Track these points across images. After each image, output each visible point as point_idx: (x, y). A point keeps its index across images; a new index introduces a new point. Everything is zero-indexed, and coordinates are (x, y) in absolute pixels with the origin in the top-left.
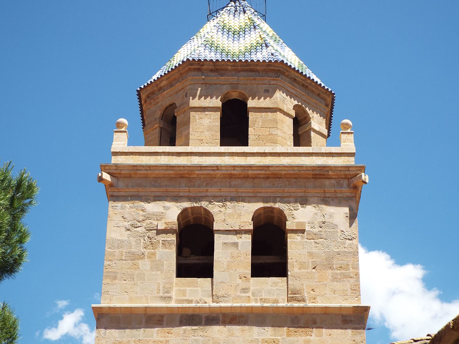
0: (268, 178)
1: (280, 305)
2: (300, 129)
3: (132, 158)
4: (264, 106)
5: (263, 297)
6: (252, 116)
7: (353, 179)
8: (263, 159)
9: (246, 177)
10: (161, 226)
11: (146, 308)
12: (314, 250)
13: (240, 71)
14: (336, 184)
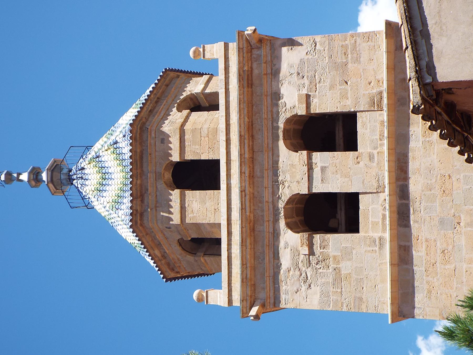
0: (252, 136)
1: (386, 118)
2: (203, 105)
3: (235, 284)
4: (178, 143)
5: (378, 137)
6: (189, 156)
7: (252, 44)
9: (252, 160)
10: (306, 250)
11: (391, 264)
12: (328, 84)
13: (142, 170)
14: (257, 62)
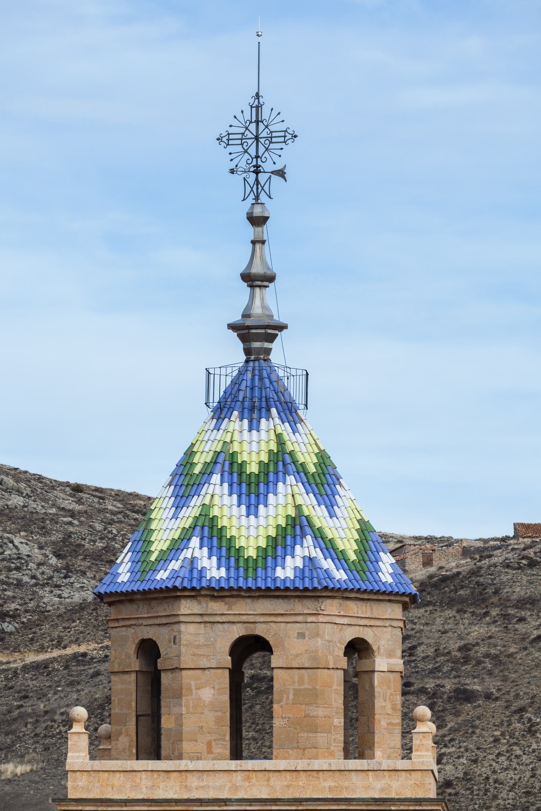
8: (294, 782)
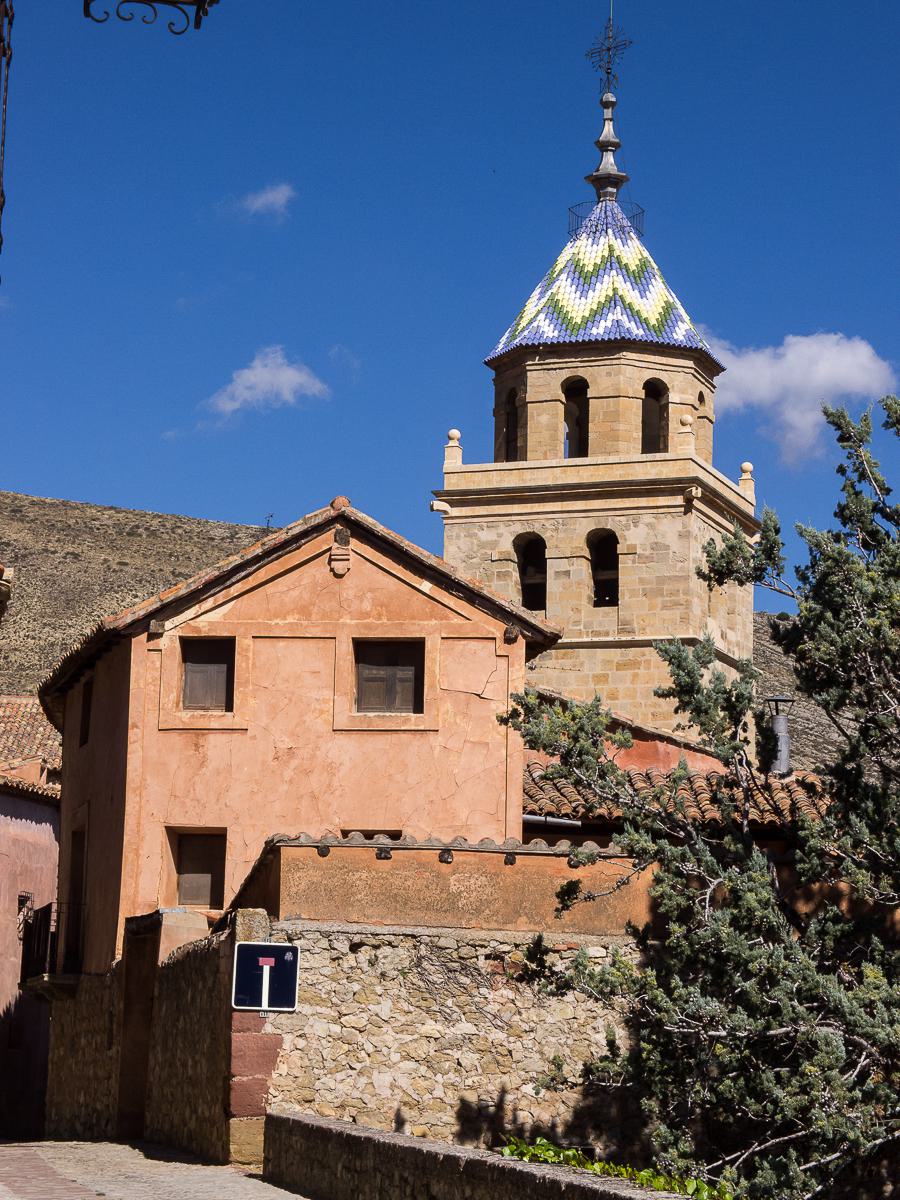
12: (644, 575)
